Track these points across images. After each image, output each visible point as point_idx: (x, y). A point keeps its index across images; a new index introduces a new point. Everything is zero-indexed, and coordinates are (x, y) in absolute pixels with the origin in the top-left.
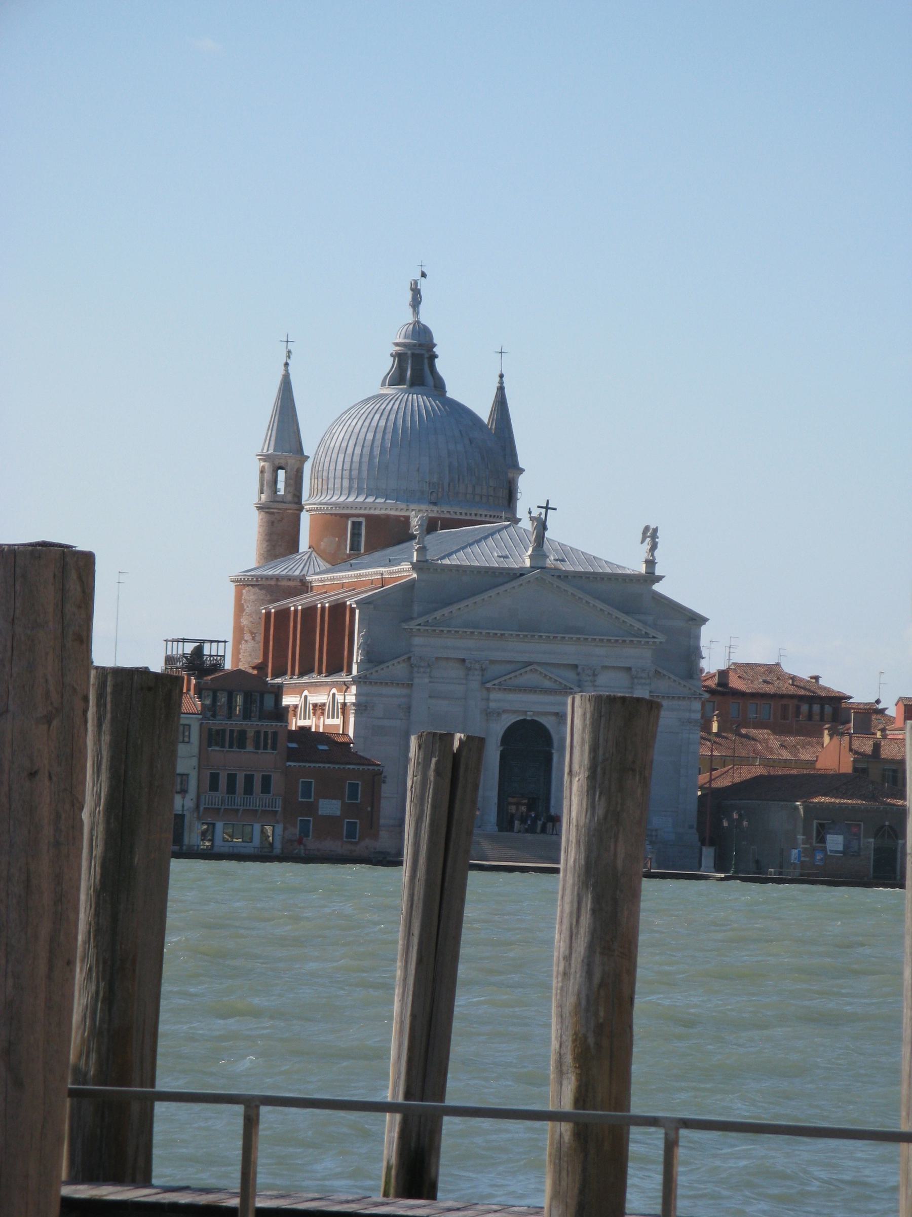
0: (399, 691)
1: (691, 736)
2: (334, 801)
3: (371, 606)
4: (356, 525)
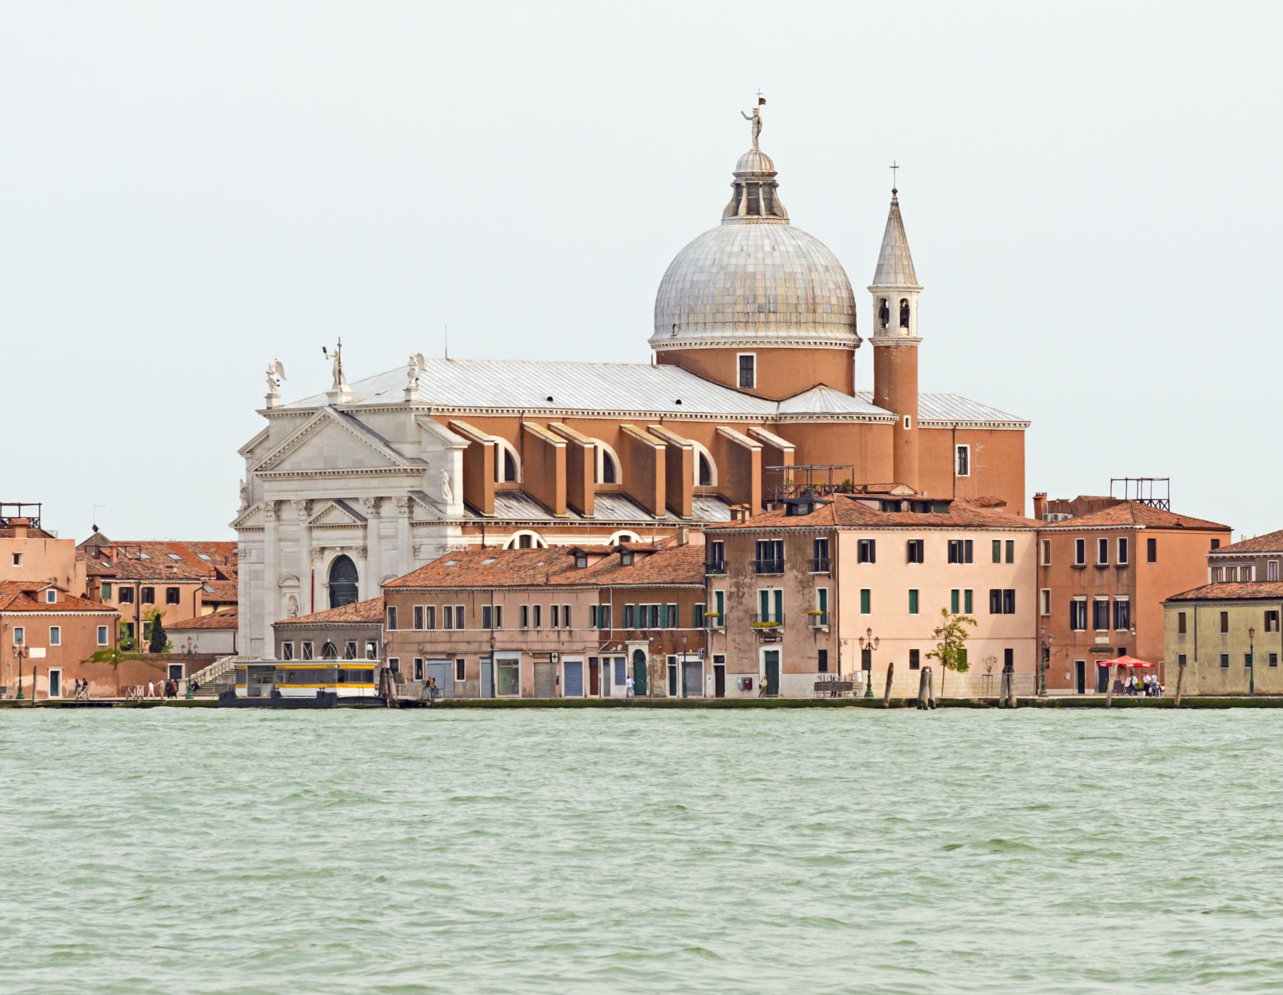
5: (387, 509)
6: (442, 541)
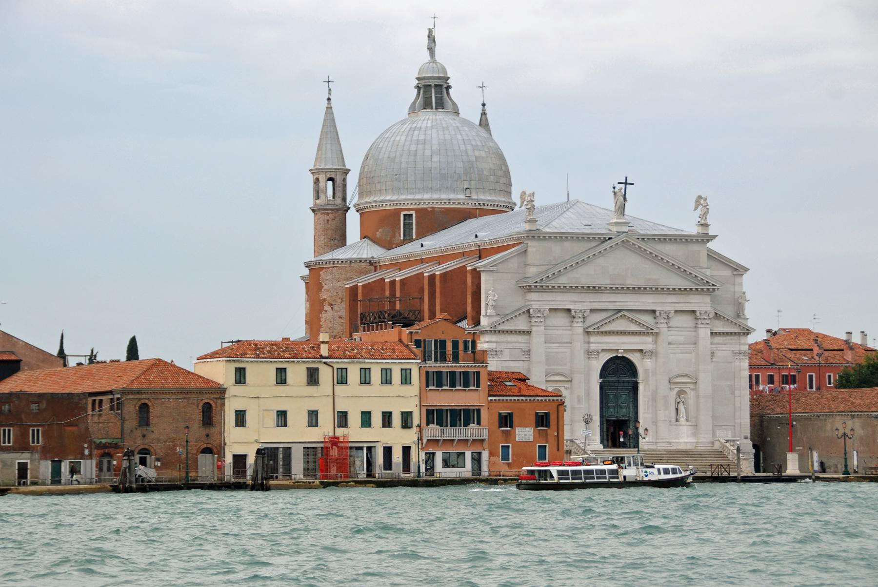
2: (527, 429)
4: (408, 217)
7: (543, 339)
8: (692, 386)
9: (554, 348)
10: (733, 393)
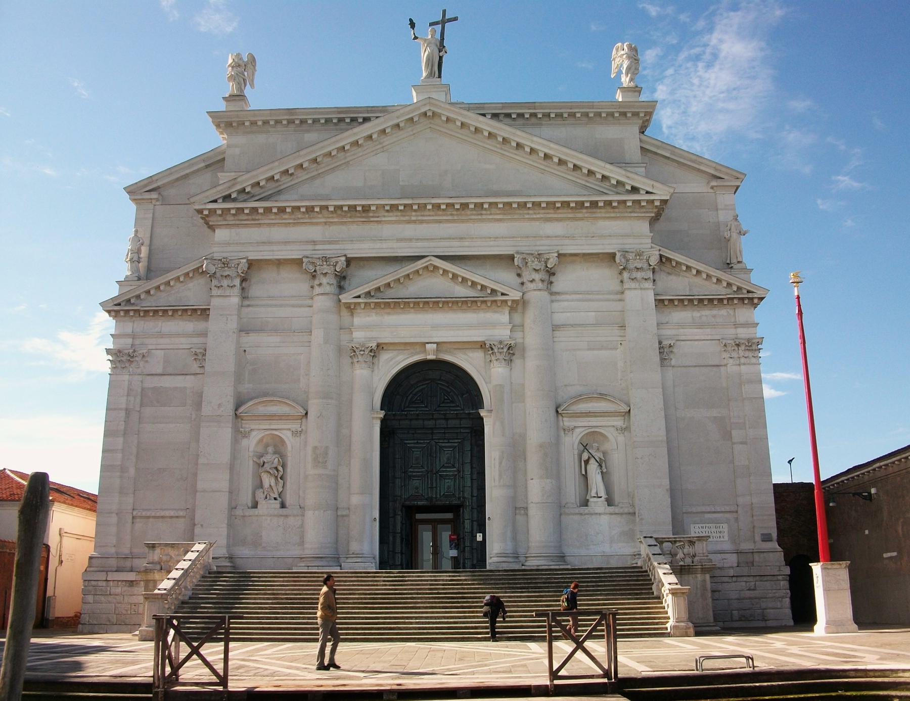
0: (189, 326)
1: (743, 368)
3: (154, 195)
5: (566, 280)
6: (743, 333)
7: (233, 325)
8: (619, 422)
9: (266, 346)
10: (727, 435)
